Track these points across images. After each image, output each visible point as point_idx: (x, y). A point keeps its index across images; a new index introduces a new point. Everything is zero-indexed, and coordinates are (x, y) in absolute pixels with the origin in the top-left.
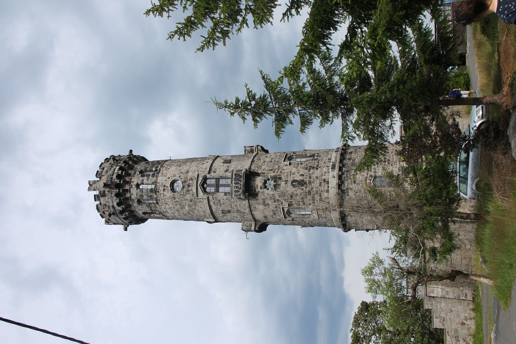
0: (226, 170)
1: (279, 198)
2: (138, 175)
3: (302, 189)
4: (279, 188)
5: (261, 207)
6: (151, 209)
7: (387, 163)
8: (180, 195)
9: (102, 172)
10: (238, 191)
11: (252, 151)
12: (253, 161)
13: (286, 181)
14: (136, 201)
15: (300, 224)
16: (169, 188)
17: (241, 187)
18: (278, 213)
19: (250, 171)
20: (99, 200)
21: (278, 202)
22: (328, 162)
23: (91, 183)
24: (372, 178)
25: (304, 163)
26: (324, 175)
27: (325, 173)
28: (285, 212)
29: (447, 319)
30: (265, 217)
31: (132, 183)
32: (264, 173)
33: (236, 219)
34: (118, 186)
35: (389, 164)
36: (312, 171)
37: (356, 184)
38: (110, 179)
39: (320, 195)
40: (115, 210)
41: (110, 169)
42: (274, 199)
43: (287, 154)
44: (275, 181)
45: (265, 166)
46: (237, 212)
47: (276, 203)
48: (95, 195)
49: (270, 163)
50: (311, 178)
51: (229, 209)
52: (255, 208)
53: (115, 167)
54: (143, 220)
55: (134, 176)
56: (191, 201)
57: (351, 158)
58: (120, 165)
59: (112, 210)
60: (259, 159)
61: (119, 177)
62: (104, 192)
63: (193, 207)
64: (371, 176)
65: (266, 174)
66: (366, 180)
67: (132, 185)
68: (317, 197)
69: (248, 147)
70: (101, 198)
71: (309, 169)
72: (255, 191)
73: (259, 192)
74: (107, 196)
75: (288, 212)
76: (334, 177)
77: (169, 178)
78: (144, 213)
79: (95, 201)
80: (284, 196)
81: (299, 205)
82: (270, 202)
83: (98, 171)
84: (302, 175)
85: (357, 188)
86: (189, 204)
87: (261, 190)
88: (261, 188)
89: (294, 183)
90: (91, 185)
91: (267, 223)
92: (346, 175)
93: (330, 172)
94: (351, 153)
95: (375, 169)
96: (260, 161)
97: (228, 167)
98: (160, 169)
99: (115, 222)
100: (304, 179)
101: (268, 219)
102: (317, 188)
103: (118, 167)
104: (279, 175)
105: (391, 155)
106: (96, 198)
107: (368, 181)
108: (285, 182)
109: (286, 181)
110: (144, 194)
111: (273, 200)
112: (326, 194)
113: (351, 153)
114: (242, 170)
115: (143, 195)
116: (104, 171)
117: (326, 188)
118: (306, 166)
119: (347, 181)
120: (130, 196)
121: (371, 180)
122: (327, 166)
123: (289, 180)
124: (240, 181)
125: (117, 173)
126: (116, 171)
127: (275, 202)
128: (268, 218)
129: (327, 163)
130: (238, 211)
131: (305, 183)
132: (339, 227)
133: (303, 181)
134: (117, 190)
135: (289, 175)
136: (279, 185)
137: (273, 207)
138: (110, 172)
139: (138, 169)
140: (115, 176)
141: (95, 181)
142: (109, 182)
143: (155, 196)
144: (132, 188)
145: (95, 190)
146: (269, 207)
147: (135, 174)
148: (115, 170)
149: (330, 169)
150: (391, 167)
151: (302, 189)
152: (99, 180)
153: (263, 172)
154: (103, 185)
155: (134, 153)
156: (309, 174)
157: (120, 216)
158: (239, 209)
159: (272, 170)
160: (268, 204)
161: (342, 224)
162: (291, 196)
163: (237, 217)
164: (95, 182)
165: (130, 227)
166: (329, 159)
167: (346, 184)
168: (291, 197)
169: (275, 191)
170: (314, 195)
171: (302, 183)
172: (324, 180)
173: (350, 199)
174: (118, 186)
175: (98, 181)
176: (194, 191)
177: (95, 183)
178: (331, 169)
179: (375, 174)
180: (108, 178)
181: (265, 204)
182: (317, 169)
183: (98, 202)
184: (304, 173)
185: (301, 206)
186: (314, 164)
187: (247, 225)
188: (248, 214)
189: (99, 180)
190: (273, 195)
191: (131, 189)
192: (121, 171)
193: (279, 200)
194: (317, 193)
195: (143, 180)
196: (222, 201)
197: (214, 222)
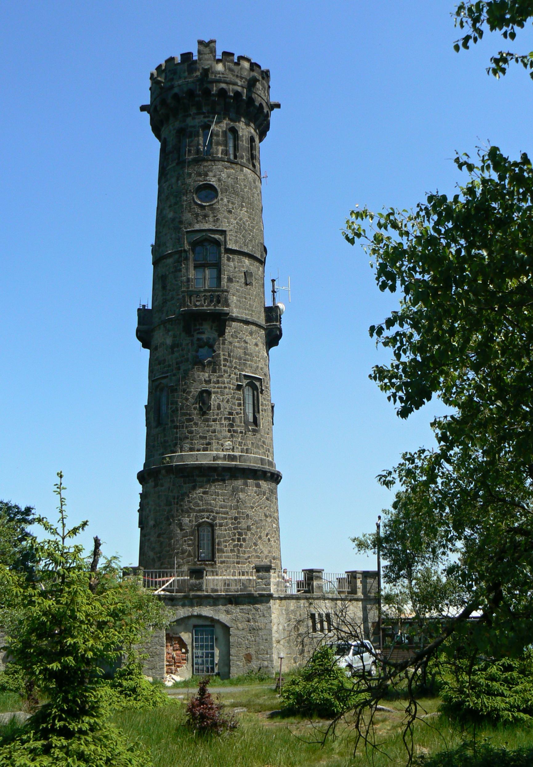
1: (181, 371)
5: (169, 341)
7: (236, 543)
9: (232, 61)
11: (269, 319)
12: (247, 322)
13: (208, 382)
16: (201, 183)
19: (226, 320)
25: (241, 409)
26: (218, 443)
34: (207, 92)
35: (235, 546)
36: (226, 422)
41: (237, 76)
42: (182, 362)
43: (259, 380)
51: (168, 287)
52: (169, 331)
60: (251, 334)
61: (223, 93)
62: (196, 70)
64: (214, 518)
66: (207, 512)
67: (208, 117)
70: (186, 64)
71: (229, 419)
72: (195, 330)
73: (193, 336)
79: (182, 55)
82: (176, 354)
83: (233, 54)
84: (219, 407)
87: (196, 339)
88: (199, 339)
94: (258, 486)
96: (247, 336)
98: (237, 164)
103: (239, 89)
104: (220, 369)
106: (187, 56)
107: (206, 514)
108: (207, 379)
109: (208, 382)
111: (179, 360)
113: (258, 486)
114: (228, 305)
116: (231, 65)
120: (190, 114)
121: (208, 518)
122: (233, 447)
123: (212, 385)
124: (209, 305)
125: (229, 89)
126: (231, 87)
127: (177, 364)
129: (240, 447)
130: (165, 302)
135: (220, 385)
136: (203, 371)
138: (230, 77)
140: (223, 86)
141: (215, 51)
142: (214, 77)
144: (205, 117)
145: (199, 52)
148: (235, 84)
150: (229, 549)
152: (217, 57)
154: (206, 67)
156: (221, 418)
160: (173, 353)
164: (213, 51)
165: (146, 116)
168: (184, 391)
175: (215, 56)
178: (229, 455)
180: (219, 74)
182: (229, 431)
184: (222, 410)
185: (170, 406)
186: (239, 426)
191: (202, 116)
192: (232, 94)
193: (180, 370)
194: (191, 432)
195: (217, 135)
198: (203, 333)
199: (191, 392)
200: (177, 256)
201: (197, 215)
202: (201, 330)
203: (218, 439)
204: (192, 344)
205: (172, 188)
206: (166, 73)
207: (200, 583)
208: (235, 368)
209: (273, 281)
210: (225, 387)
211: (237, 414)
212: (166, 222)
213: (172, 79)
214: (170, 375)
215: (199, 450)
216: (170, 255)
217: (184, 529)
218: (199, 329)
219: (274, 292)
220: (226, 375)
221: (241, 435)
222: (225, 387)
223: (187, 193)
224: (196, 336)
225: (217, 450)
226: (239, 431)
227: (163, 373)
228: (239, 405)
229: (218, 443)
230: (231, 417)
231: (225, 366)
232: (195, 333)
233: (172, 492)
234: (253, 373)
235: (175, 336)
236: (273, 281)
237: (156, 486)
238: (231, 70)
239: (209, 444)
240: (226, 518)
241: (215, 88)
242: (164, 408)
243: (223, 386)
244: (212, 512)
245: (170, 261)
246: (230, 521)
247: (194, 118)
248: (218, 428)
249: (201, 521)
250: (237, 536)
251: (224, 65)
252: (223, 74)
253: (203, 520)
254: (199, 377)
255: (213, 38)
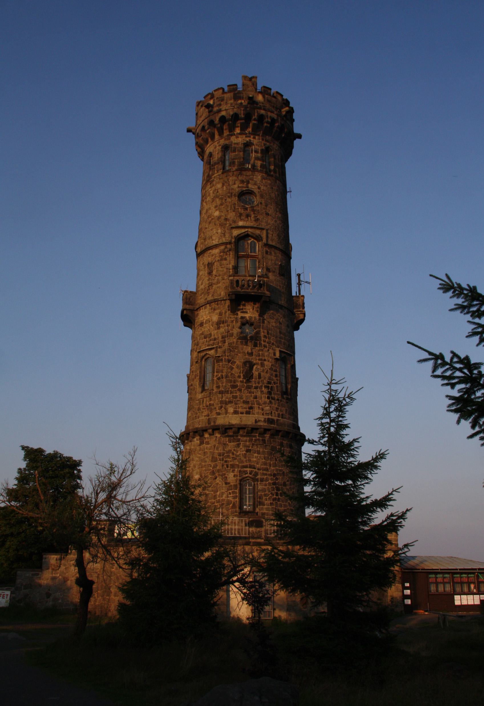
0: (269, 269)
1: (227, 343)
2: (264, 145)
3: (239, 377)
4: (242, 343)
5: (215, 318)
6: (215, 164)
7: (275, 496)
8: (235, 204)
10: (237, 286)
13: (251, 354)
14: (227, 142)
15: (192, 374)
17: (244, 289)
18: (206, 342)
20: (230, 91)
21: (221, 341)
22: (279, 415)
23: (253, 80)
24: (254, 475)
26: (259, 408)
27: (263, 410)
28: (207, 352)
29: (55, 574)
30: (202, 324)
31: (252, 136)
32: (263, 322)
33: (200, 283)
35: (274, 499)
37: (244, 452)
38: (259, 106)
39: (230, 402)
40: (215, 113)
41: (273, 107)
44: (252, 338)
45: (274, 324)
46: (209, 283)
47: (220, 339)
48: (236, 85)
49: (278, 330)
50: (255, 389)
51: (214, 273)
52: (215, 310)
53: (275, 113)
54: (201, 154)
55: (263, 140)
56: (226, 219)
57: (283, 446)
58: (279, 120)
59: (215, 109)
63: (218, 222)
64: (256, 474)
65: (263, 326)
66: (251, 467)
67: (250, 137)
68: (226, 397)
69: (303, 301)
70: (232, 94)
71: (267, 387)
73: (237, 314)
74: (235, 102)
75: (208, 356)
76: (256, 421)
77: (259, 188)
78: (211, 155)
79: (228, 86)
80: (231, 351)
81: (217, 372)
82: (222, 330)
83: (270, 89)
85: (240, 454)
86: (222, 216)
89: (248, 365)
90: (251, 79)
91: (193, 326)
92: (259, 439)
93: (263, 416)
95: (267, 480)
97: (274, 272)
99: (199, 115)
100: (253, 380)
101: (198, 328)
102: (241, 398)
104: (260, 344)
105: (287, 504)
106: (233, 88)
107: (248, 469)
108: (250, 351)
110: (237, 153)
112: (231, 410)
115: (235, 152)
117: (240, 410)
118: (272, 382)
119: (249, 441)
121: (250, 473)
125: (267, 116)
126: (269, 114)
127: (223, 337)
128: (201, 328)
129: (277, 413)
130: (211, 285)
131: (248, 381)
132: (187, 427)
133: (252, 377)
134: (243, 116)
136: (246, 344)
137: (214, 335)
138: (268, 106)
139: (274, 145)
140: (262, 112)
141: (256, 86)
143: (234, 169)
144: (246, 137)
145: (243, 85)
146: (216, 330)
147: (266, 141)
148: (272, 112)
149: (268, 417)
151: (239, 377)
152: (258, 91)
153: (265, 321)
155: (297, 142)
156: (262, 386)
157: (206, 120)
158: (214, 287)
159: (268, 333)
160: (219, 328)
161: (189, 433)
162: (231, 360)
163: (202, 284)
164: (255, 85)
166: (282, 415)
167: (245, 438)
169: (237, 337)
170: (231, 394)
171: (248, 376)
172: (251, 408)
173: (225, 444)
174: (248, 117)
175: (256, 89)
176: (241, 223)
177: (253, 84)
178: (268, 418)
179: (259, 480)
181: (219, 323)
182: (268, 398)
183: (226, 89)
185: (216, 374)
186: (275, 394)
187: (191, 299)
188: (206, 299)
189: (258, 91)
190: (232, 335)
191: (244, 136)
193: (225, 343)
196: (224, 262)
197: (196, 252)
198: (246, 312)
199: (235, 362)
200: (223, 247)
201: (241, 215)
202: (244, 310)
203: (259, 404)
204: (237, 322)
205: (218, 192)
206: (214, 100)
207: (259, 532)
208: (273, 344)
209: (299, 275)
210: (265, 360)
211: (275, 383)
212: (212, 219)
213: (220, 105)
214: (217, 347)
215: (242, 413)
216: (216, 246)
217: (229, 483)
218: (242, 309)
219: (299, 284)
220: (266, 349)
221: (277, 402)
222: (265, 360)
223: (232, 196)
224: (240, 315)
225: (258, 413)
226: (276, 398)
227: (208, 346)
228: (276, 376)
229: (259, 408)
230: (270, 385)
231: (265, 341)
232: (239, 313)
233: (217, 449)
234: (286, 350)
235: (220, 314)
236: (299, 275)
237: (202, 443)
238: (269, 101)
239: (251, 408)
240: (266, 474)
241: (256, 114)
242: (209, 377)
243: (263, 358)
244: (254, 468)
245: (216, 251)
246: (270, 477)
247: (237, 137)
248: (259, 394)
249: (244, 476)
250: (276, 491)
251: (264, 97)
252: (262, 103)
253: (247, 475)
254: (242, 350)
255: (255, 75)
